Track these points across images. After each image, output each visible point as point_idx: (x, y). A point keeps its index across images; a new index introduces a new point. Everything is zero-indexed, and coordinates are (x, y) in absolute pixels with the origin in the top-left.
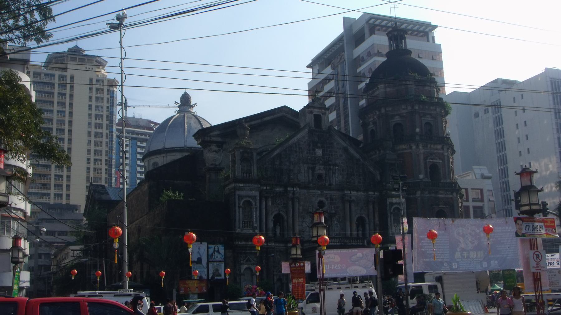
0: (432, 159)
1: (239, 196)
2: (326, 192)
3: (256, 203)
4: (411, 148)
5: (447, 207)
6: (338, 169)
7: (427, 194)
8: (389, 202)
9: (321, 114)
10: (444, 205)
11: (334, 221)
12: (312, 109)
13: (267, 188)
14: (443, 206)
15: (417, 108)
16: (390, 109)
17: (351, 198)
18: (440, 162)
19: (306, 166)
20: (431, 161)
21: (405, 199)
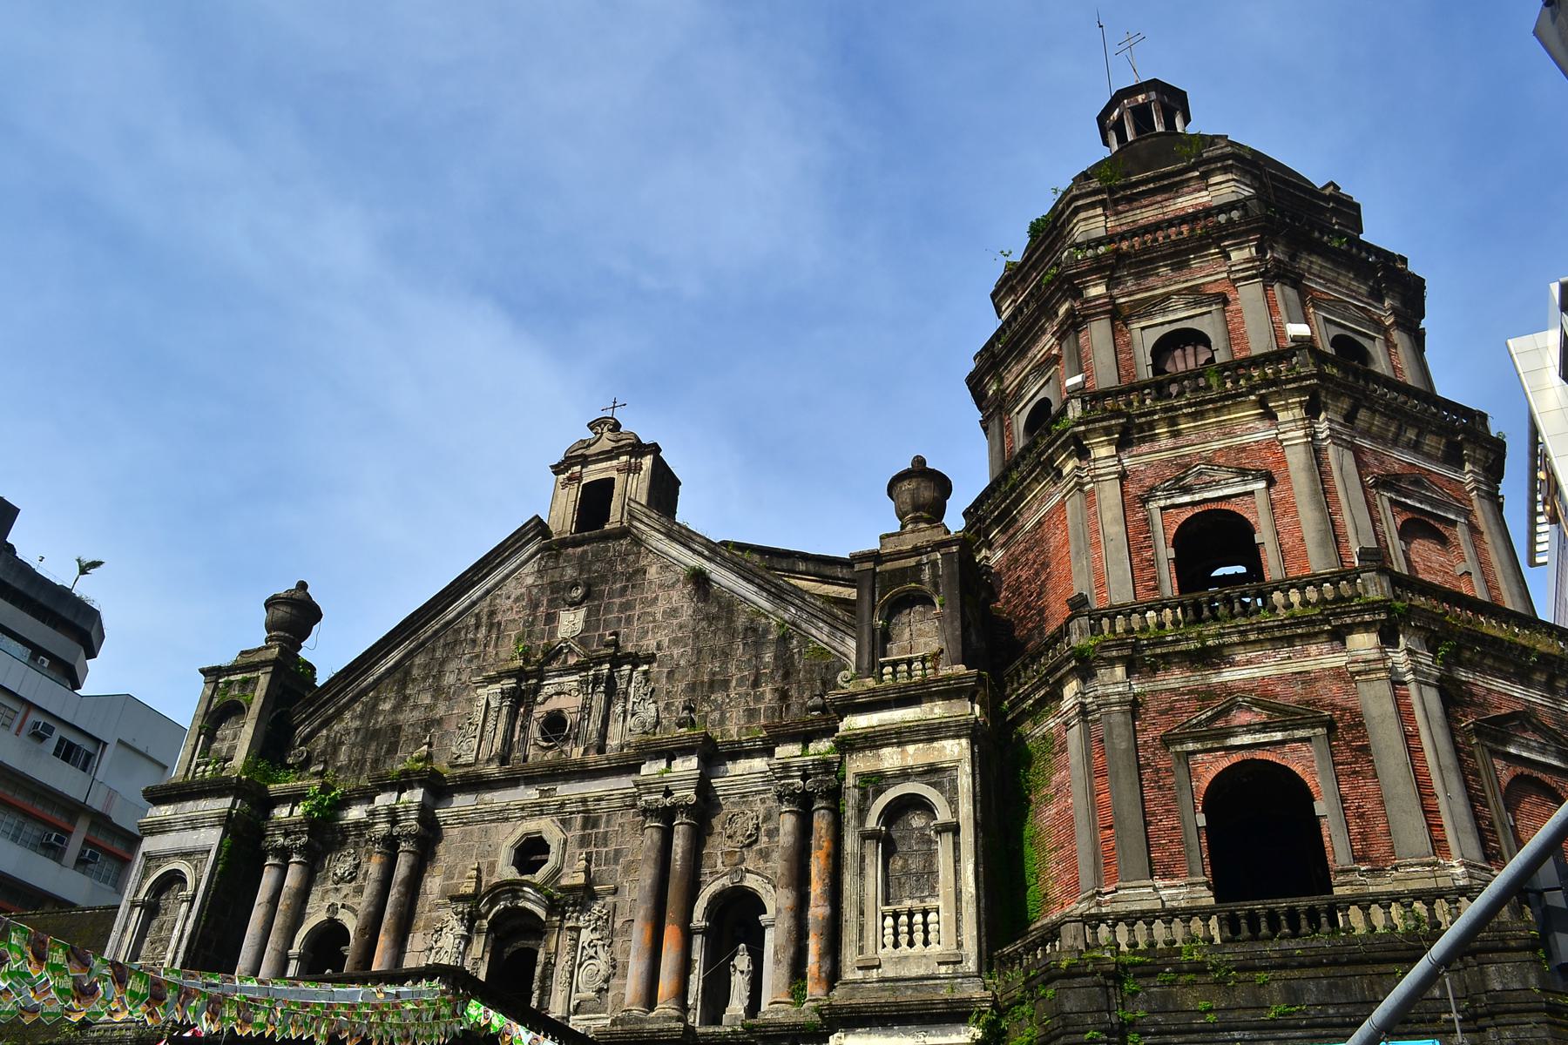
0: (1187, 490)
1: (149, 857)
2: (568, 791)
3: (198, 883)
4: (1059, 474)
6: (645, 673)
8: (857, 775)
9: (614, 474)
10: (1265, 727)
11: (578, 930)
12: (577, 468)
14: (1262, 738)
17: (668, 793)
18: (1252, 493)
19: (496, 688)
20: (1187, 499)
21: (964, 742)
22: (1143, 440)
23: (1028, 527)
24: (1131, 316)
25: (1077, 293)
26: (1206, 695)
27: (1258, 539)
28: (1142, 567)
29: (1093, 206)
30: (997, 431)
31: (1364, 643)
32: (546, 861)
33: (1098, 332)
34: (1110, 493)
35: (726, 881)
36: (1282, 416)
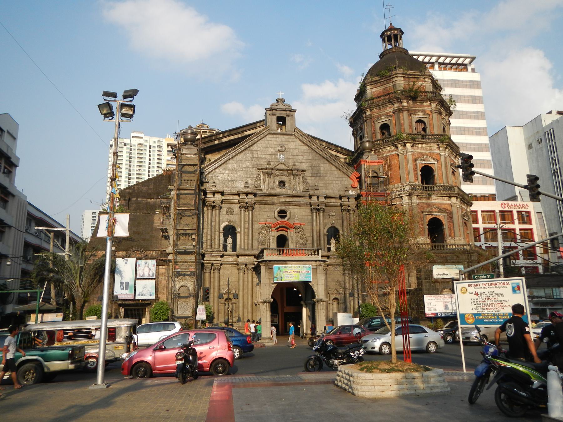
0: (424, 160)
4: (397, 148)
5: (443, 214)
7: (415, 200)
10: (439, 212)
13: (214, 196)
15: (405, 104)
16: (376, 110)
20: (423, 162)
22: (416, 146)
23: (385, 155)
24: (412, 114)
25: (401, 102)
26: (429, 205)
27: (435, 174)
28: (416, 175)
29: (401, 76)
30: (370, 125)
31: (453, 199)
32: (286, 216)
33: (405, 114)
34: (410, 158)
35: (330, 226)
36: (441, 149)
